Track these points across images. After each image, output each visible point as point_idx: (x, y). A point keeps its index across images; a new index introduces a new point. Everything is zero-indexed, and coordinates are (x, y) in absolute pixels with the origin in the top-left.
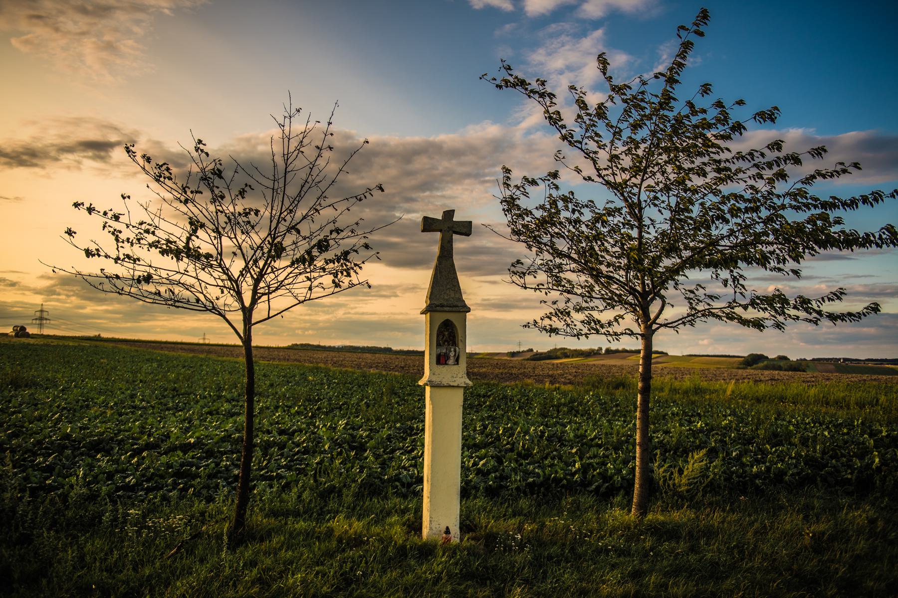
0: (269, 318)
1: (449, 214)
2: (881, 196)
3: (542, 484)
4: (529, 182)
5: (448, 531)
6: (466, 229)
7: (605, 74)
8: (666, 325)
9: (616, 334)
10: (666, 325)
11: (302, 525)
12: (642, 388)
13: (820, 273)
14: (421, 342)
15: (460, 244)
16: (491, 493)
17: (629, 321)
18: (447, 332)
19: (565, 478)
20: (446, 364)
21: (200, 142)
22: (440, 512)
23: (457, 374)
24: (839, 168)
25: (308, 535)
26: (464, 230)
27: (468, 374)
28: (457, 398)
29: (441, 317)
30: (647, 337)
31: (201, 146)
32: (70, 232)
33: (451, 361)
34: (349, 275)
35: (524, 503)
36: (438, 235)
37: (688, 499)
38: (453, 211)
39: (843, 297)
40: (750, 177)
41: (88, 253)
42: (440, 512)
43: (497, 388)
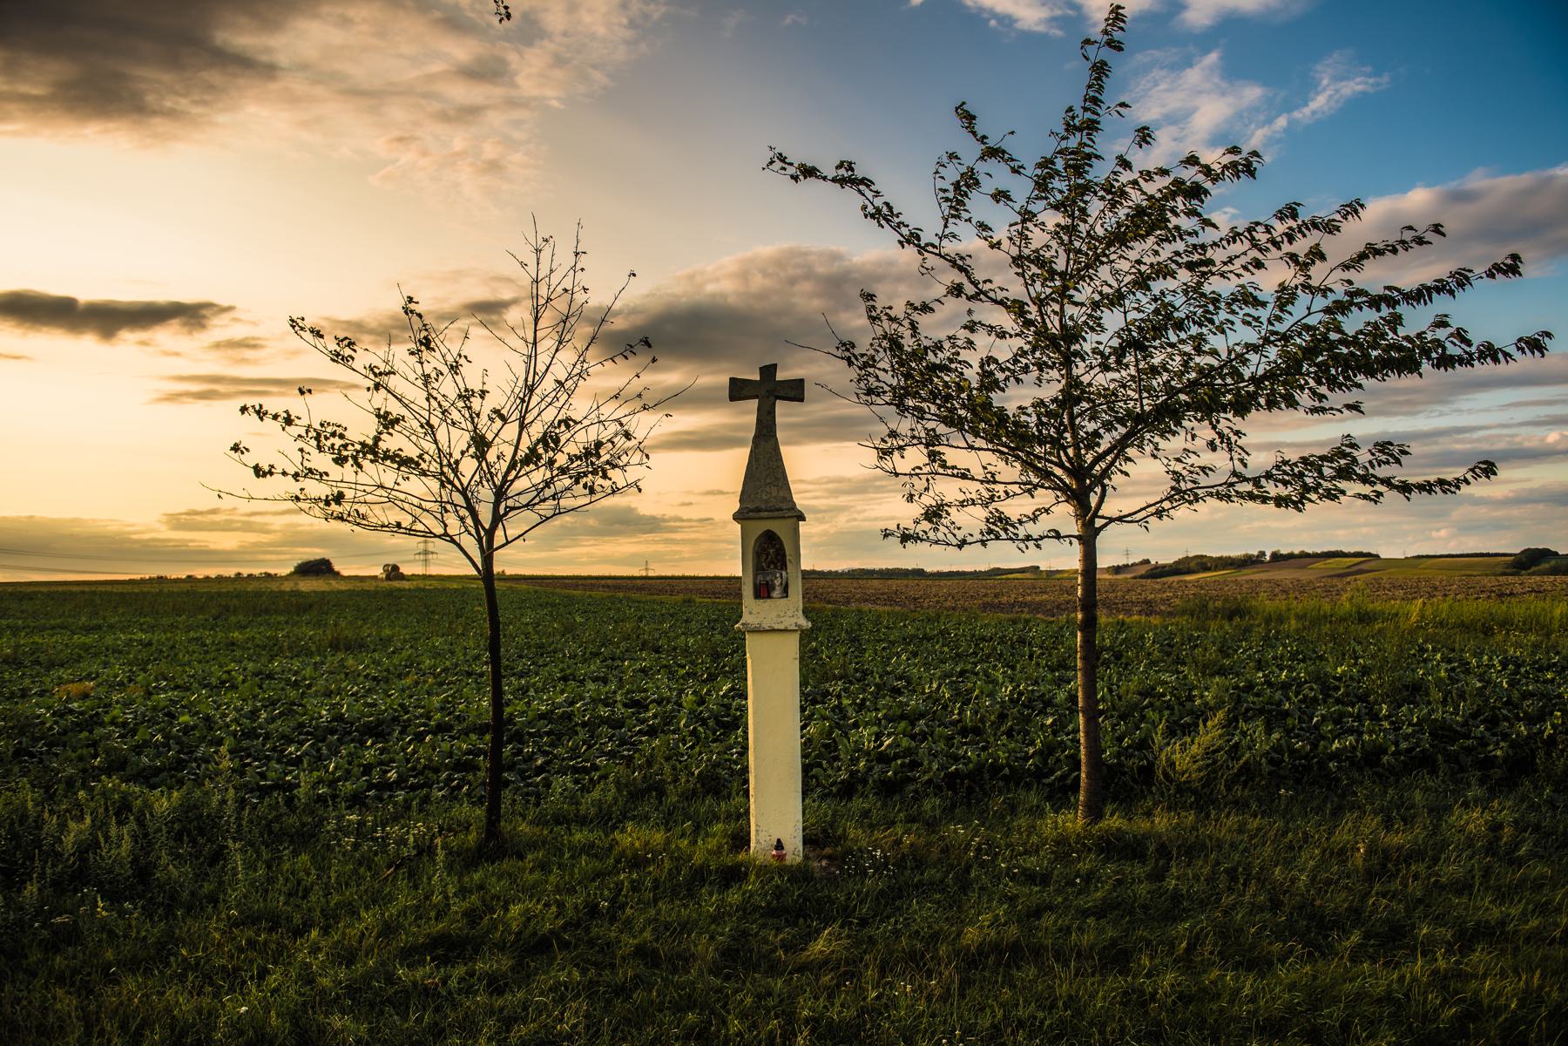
0: (508, 542)
1: (769, 371)
2: (1467, 279)
3: (970, 775)
4: (916, 309)
5: (779, 845)
6: (795, 391)
7: (974, 133)
8: (1120, 519)
9: (1028, 538)
10: (1120, 519)
11: (579, 837)
12: (1083, 620)
13: (1381, 414)
14: (731, 565)
15: (785, 412)
16: (888, 789)
17: (1064, 516)
18: (770, 554)
19: (1008, 765)
20: (769, 597)
21: (410, 300)
22: (776, 816)
23: (788, 611)
24: (1408, 236)
25: (588, 849)
26: (792, 394)
27: (806, 612)
28: (791, 645)
29: (761, 527)
30: (1088, 539)
31: (412, 306)
32: (236, 448)
33: (776, 594)
34: (605, 476)
35: (930, 805)
36: (754, 404)
37: (1199, 796)
38: (775, 366)
39: (1403, 459)
40: (1245, 268)
41: (258, 471)
42: (776, 816)
43: (858, 626)
